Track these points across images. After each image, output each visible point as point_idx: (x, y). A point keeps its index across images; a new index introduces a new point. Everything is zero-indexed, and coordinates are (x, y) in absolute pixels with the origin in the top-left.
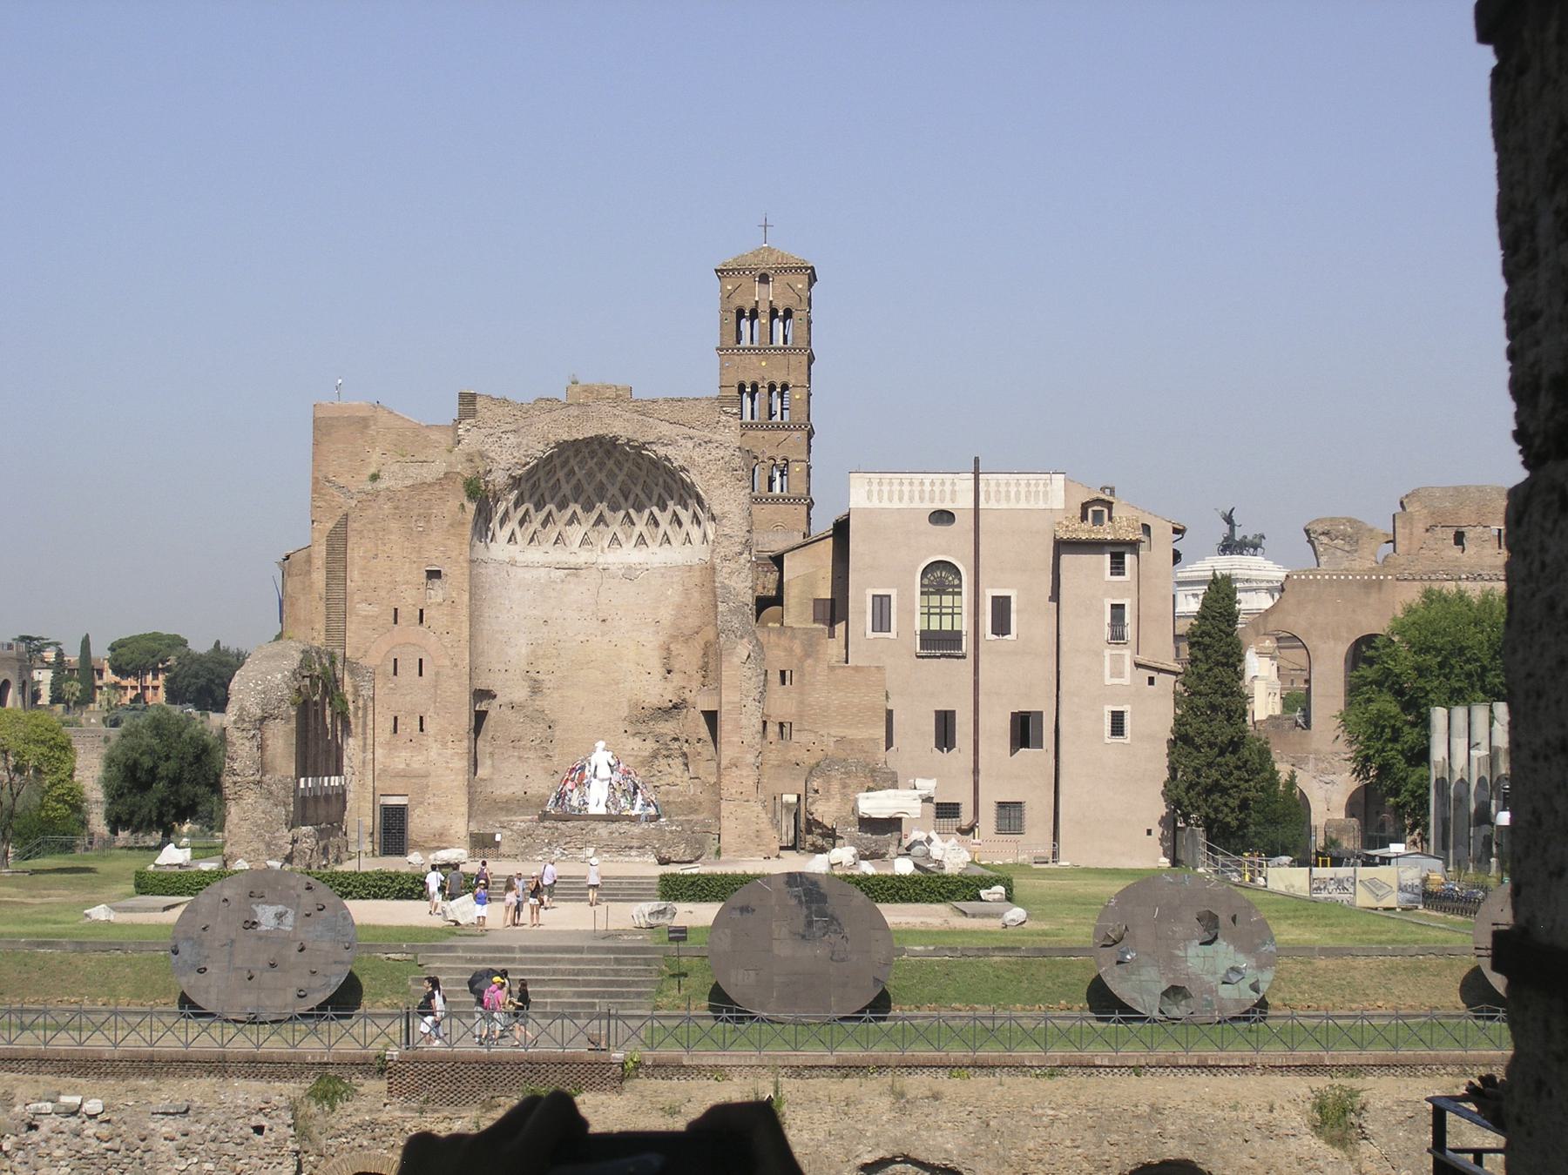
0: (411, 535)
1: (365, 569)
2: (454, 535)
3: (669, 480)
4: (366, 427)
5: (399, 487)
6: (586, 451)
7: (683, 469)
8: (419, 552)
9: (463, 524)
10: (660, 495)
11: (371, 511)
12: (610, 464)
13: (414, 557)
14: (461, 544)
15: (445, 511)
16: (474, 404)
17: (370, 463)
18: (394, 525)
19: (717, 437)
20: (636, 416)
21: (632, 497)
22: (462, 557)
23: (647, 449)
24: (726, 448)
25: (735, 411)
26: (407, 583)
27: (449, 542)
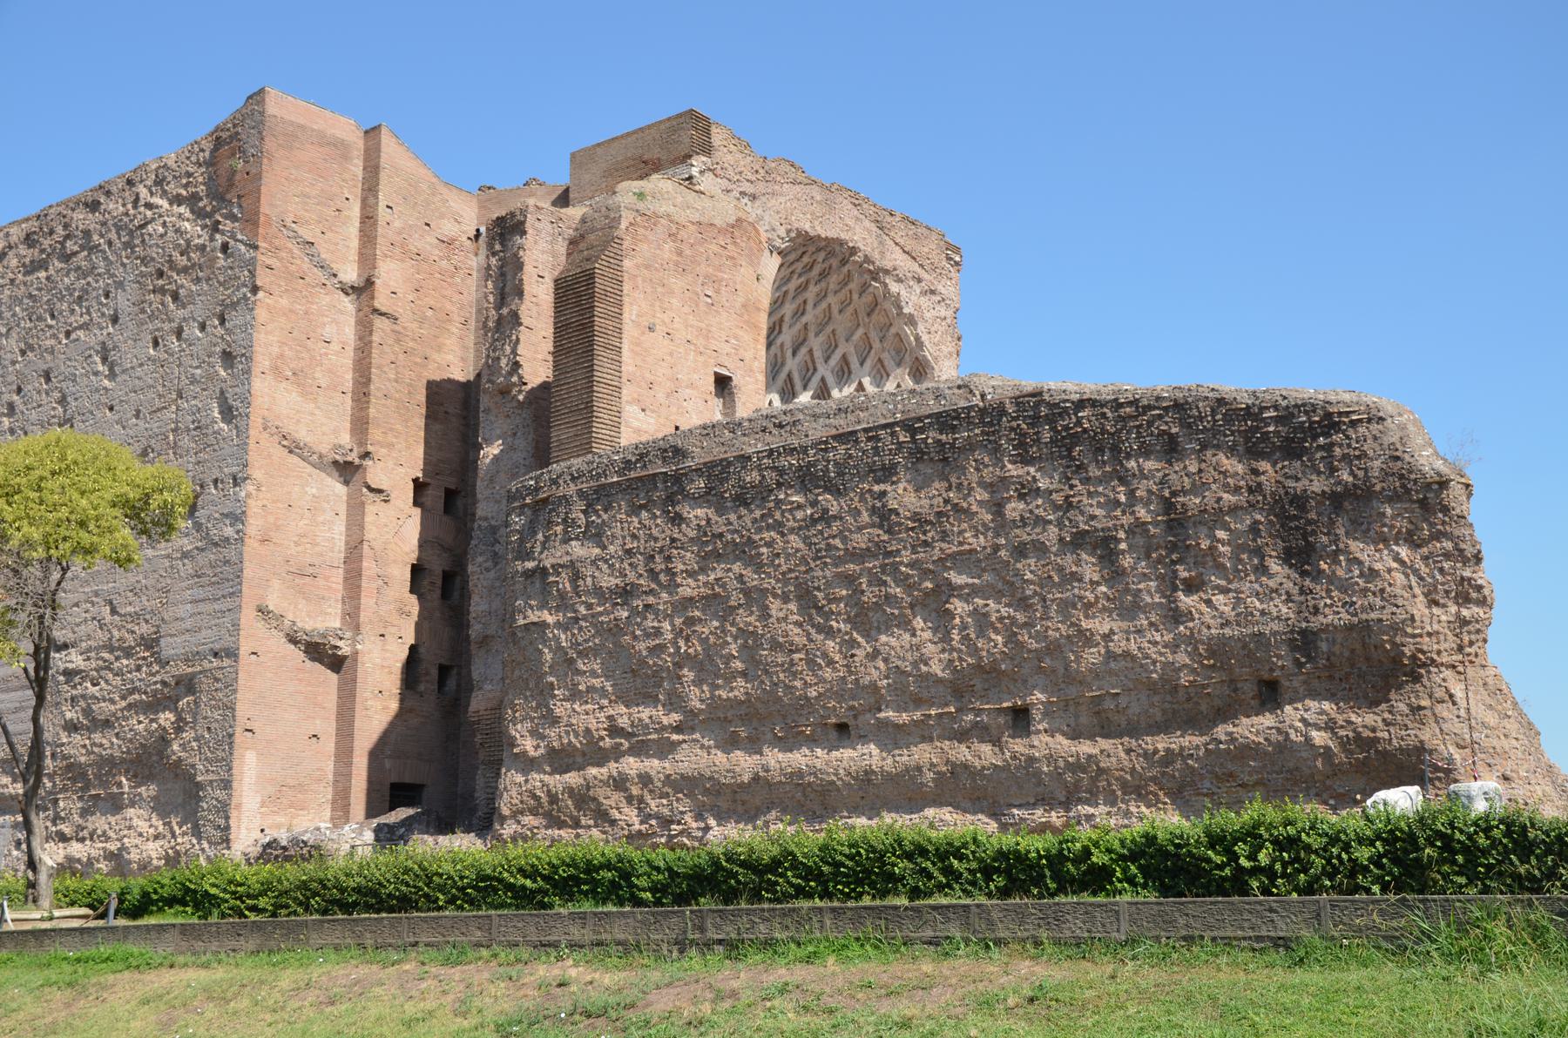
0: (697, 305)
1: (638, 345)
2: (747, 322)
3: (874, 336)
4: (346, 157)
5: (682, 220)
6: (806, 259)
7: (911, 320)
8: (707, 338)
9: (759, 309)
10: (844, 358)
11: (645, 246)
12: (811, 293)
13: (701, 342)
14: (756, 340)
15: (738, 279)
16: (708, 133)
17: (348, 217)
18: (677, 283)
19: (940, 288)
20: (873, 227)
21: (803, 350)
22: (756, 364)
23: (875, 279)
24: (948, 306)
25: (958, 259)
26: (692, 386)
27: (741, 333)
